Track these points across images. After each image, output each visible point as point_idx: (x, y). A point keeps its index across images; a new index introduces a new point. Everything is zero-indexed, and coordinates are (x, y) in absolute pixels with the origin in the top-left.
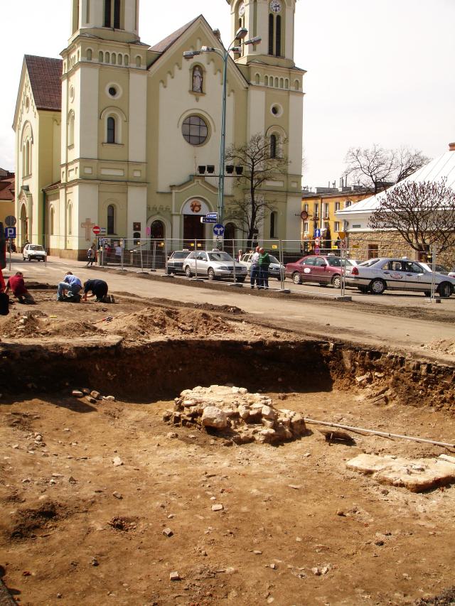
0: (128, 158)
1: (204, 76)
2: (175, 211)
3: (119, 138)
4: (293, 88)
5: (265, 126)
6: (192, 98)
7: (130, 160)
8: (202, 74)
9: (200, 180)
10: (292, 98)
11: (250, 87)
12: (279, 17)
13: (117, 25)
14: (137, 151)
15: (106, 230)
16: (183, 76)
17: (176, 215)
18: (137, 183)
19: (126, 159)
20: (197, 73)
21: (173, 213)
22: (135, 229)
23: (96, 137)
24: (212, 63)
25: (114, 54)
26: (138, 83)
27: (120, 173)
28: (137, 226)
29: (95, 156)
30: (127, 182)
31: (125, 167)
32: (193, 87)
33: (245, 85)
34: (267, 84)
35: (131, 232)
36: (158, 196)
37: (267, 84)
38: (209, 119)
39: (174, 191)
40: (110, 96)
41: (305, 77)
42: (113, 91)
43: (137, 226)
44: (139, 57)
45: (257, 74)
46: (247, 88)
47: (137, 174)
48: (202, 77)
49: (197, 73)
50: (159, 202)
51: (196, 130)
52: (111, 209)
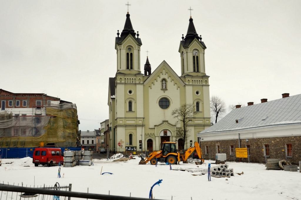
0: (137, 116)
1: (167, 83)
2: (156, 135)
3: (133, 109)
4: (204, 84)
5: (193, 99)
6: (162, 91)
7: (138, 117)
8: (166, 82)
9: (166, 123)
10: (204, 87)
11: (186, 85)
12: (197, 57)
13: (132, 68)
14: (140, 113)
15: (129, 144)
16: (158, 84)
17: (157, 136)
18: (139, 126)
19: (135, 116)
20: (164, 82)
21: (156, 136)
22: (140, 143)
23: (124, 110)
24: (170, 78)
26: (140, 88)
27: (134, 122)
28: (140, 142)
29: (123, 116)
30: (136, 126)
31: (135, 119)
33: (184, 84)
34: (193, 83)
35: (138, 144)
36: (150, 130)
37: (193, 83)
38: (170, 99)
39: (156, 127)
41: (209, 79)
42: (130, 92)
43: (140, 142)
44: (140, 79)
45: (189, 80)
46: (185, 86)
47: (140, 122)
48: (166, 84)
49: (164, 82)
50: (150, 132)
51: (164, 103)
52: (131, 136)
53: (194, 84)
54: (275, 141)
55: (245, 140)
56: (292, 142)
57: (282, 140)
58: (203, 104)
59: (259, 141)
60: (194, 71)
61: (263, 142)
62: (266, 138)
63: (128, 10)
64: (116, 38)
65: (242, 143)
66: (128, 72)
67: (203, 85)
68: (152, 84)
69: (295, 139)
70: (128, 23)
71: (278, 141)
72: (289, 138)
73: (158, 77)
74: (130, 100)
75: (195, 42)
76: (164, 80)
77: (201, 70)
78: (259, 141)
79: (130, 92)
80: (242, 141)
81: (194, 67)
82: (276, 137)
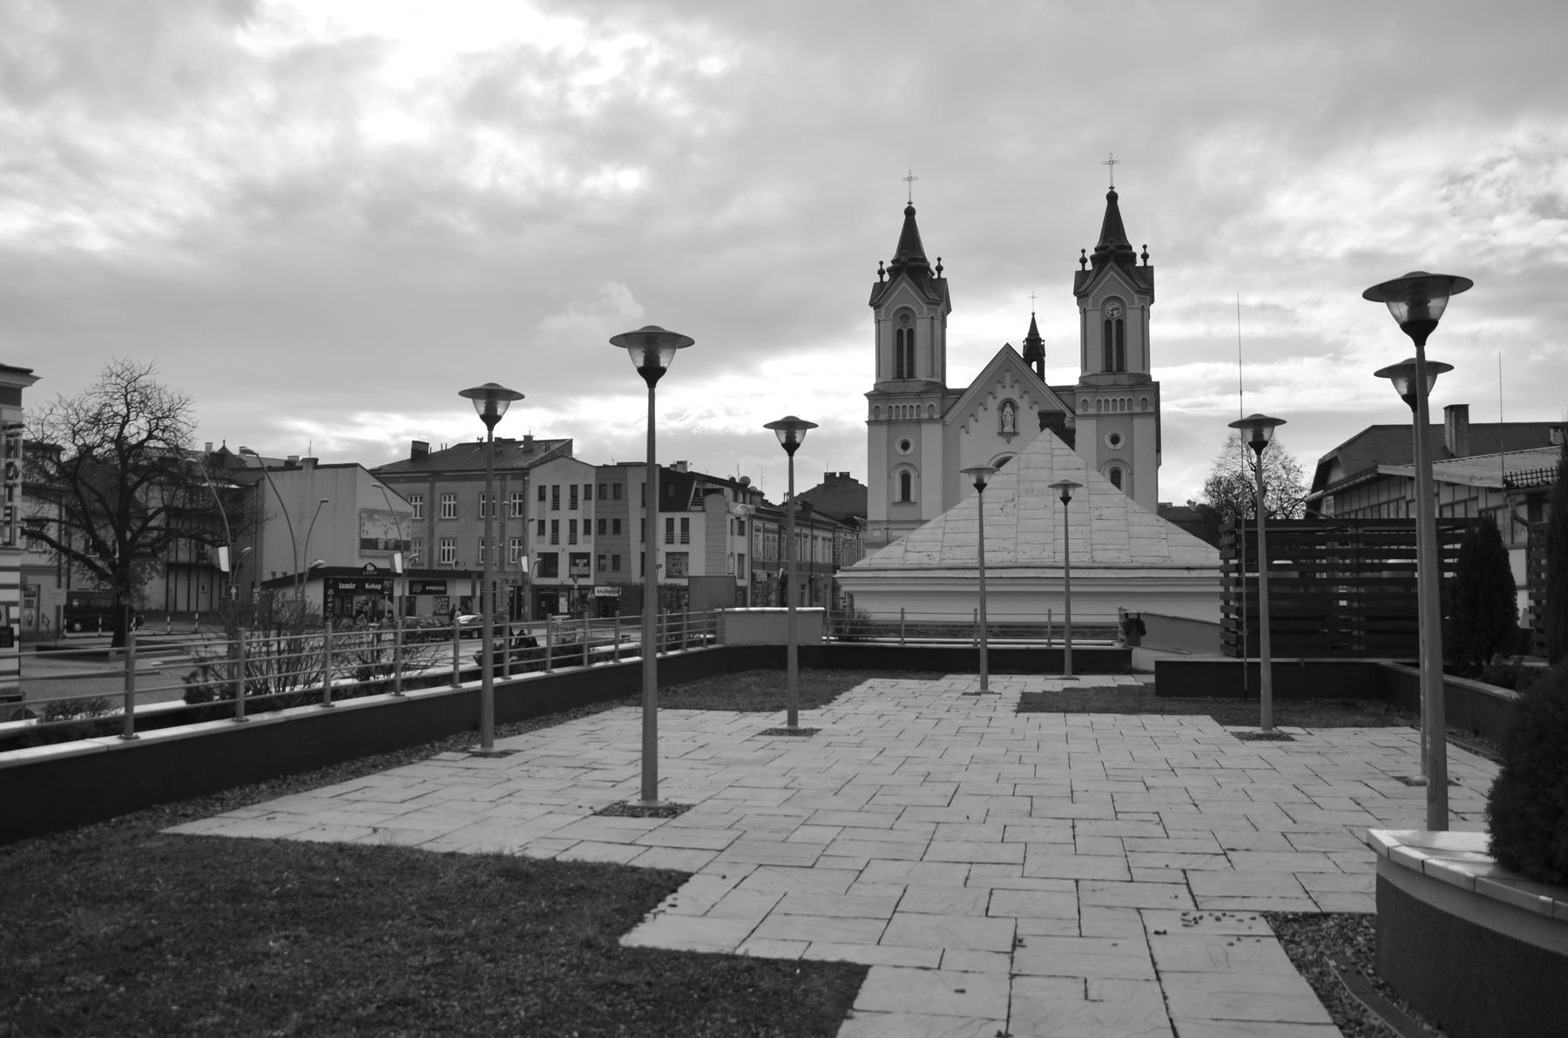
3: (913, 498)
4: (1138, 409)
6: (1002, 440)
12: (1120, 323)
13: (911, 374)
20: (1008, 409)
24: (1026, 397)
25: (904, 407)
32: (1003, 426)
34: (1099, 409)
37: (1099, 409)
40: (901, 451)
49: (1008, 409)
53: (1103, 412)
58: (1132, 474)
60: (1108, 369)
63: (910, 194)
64: (875, 284)
66: (900, 386)
67: (1132, 415)
68: (972, 420)
70: (910, 237)
73: (990, 398)
74: (904, 468)
75: (1112, 273)
76: (1010, 403)
77: (1132, 366)
79: (905, 446)
81: (1108, 356)
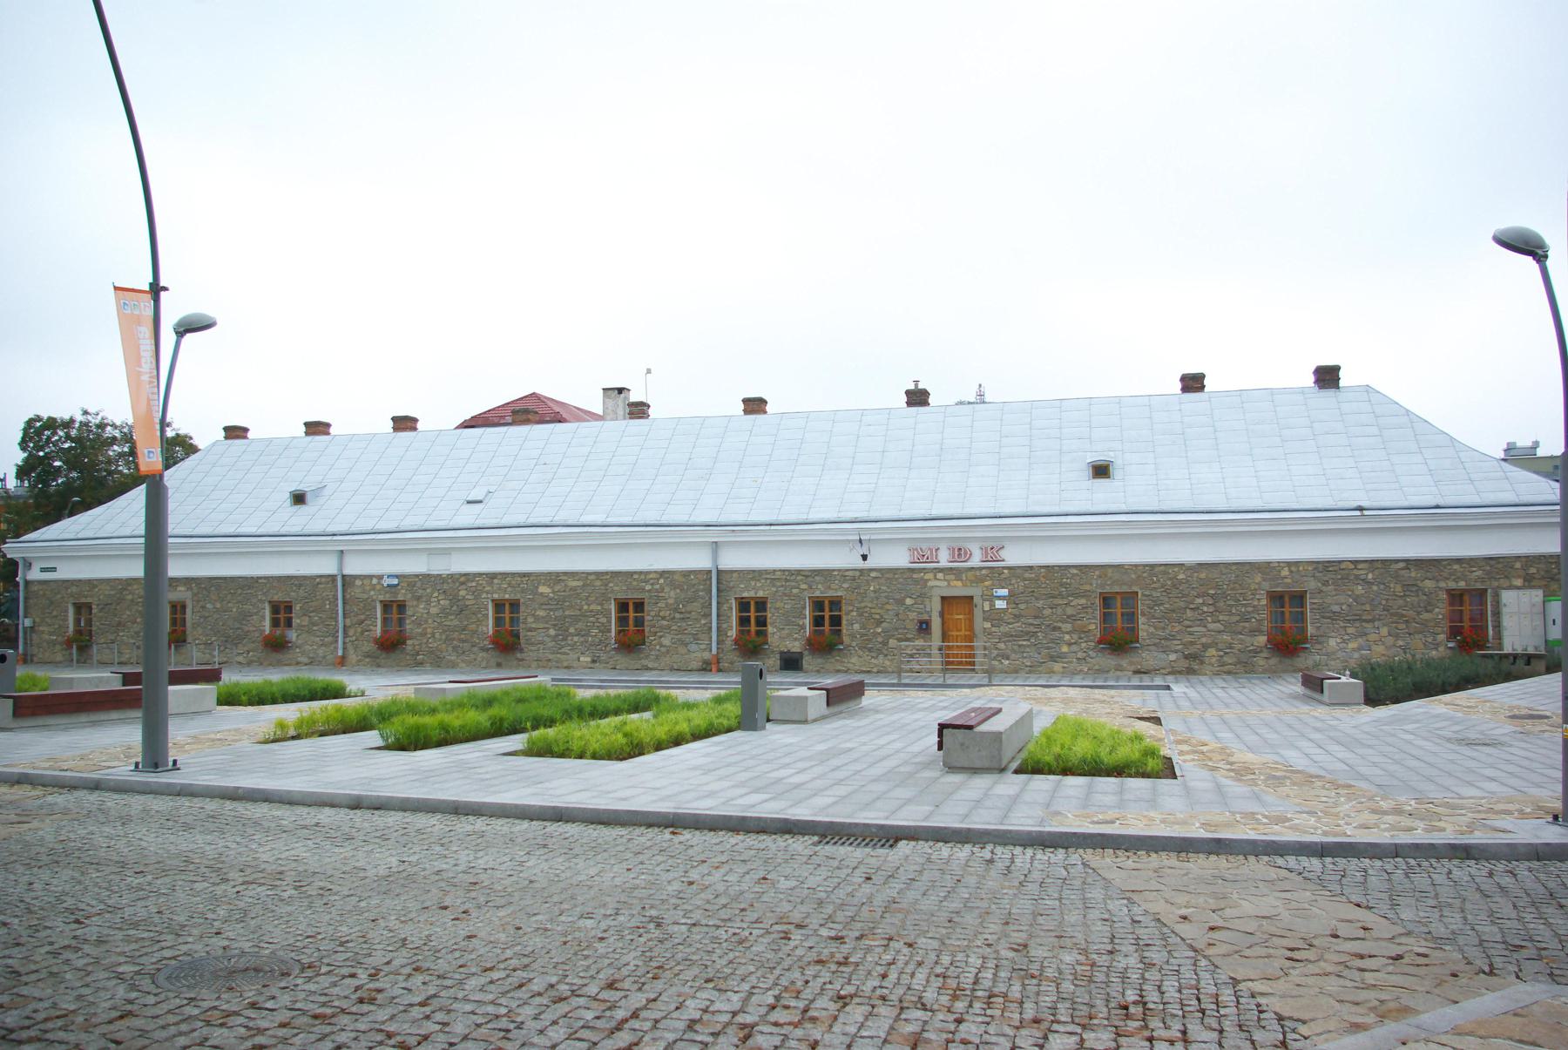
54: (557, 588)
55: (375, 581)
56: (649, 591)
57: (598, 583)
59: (463, 583)
61: (488, 588)
62: (505, 575)
65: (356, 592)
69: (661, 581)
71: (573, 589)
72: (636, 576)
78: (463, 583)
80: (358, 582)
82: (565, 573)
